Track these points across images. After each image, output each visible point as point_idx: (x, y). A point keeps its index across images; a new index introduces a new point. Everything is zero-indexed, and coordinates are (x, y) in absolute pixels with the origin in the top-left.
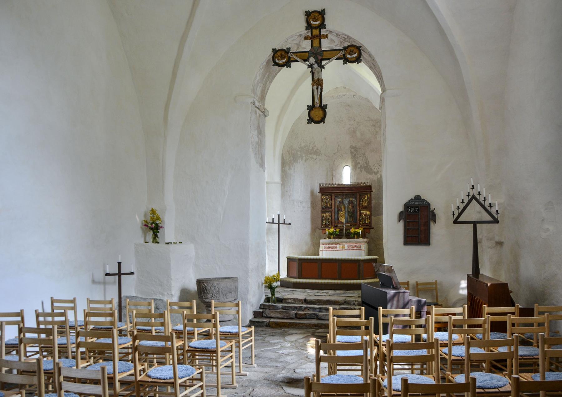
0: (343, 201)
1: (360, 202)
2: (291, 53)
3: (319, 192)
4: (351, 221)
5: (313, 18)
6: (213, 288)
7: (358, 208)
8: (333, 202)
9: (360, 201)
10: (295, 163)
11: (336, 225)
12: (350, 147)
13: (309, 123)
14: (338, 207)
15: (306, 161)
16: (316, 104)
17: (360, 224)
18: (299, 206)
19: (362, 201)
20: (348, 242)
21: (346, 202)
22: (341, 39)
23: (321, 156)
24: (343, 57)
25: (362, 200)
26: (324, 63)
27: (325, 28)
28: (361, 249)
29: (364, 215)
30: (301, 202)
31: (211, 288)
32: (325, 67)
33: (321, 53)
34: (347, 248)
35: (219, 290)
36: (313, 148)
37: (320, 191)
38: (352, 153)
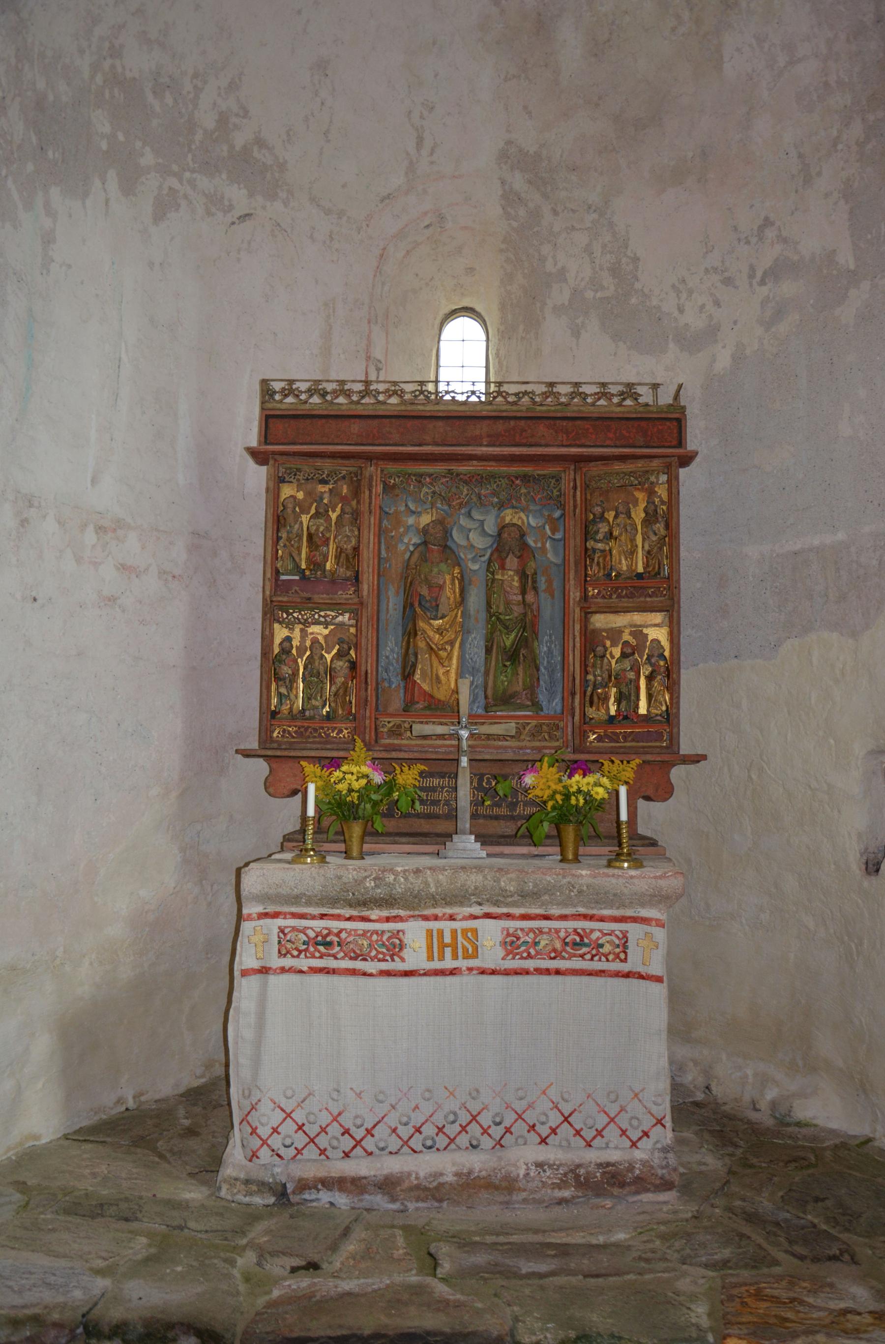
0: (447, 533)
1: (590, 544)
8: (369, 538)
9: (587, 535)
12: (503, 156)
15: (160, 212)
18: (79, 560)
19: (610, 536)
20: (503, 892)
23: (286, 204)
34: (501, 952)
36: (223, 120)
37: (266, 436)
38: (511, 198)
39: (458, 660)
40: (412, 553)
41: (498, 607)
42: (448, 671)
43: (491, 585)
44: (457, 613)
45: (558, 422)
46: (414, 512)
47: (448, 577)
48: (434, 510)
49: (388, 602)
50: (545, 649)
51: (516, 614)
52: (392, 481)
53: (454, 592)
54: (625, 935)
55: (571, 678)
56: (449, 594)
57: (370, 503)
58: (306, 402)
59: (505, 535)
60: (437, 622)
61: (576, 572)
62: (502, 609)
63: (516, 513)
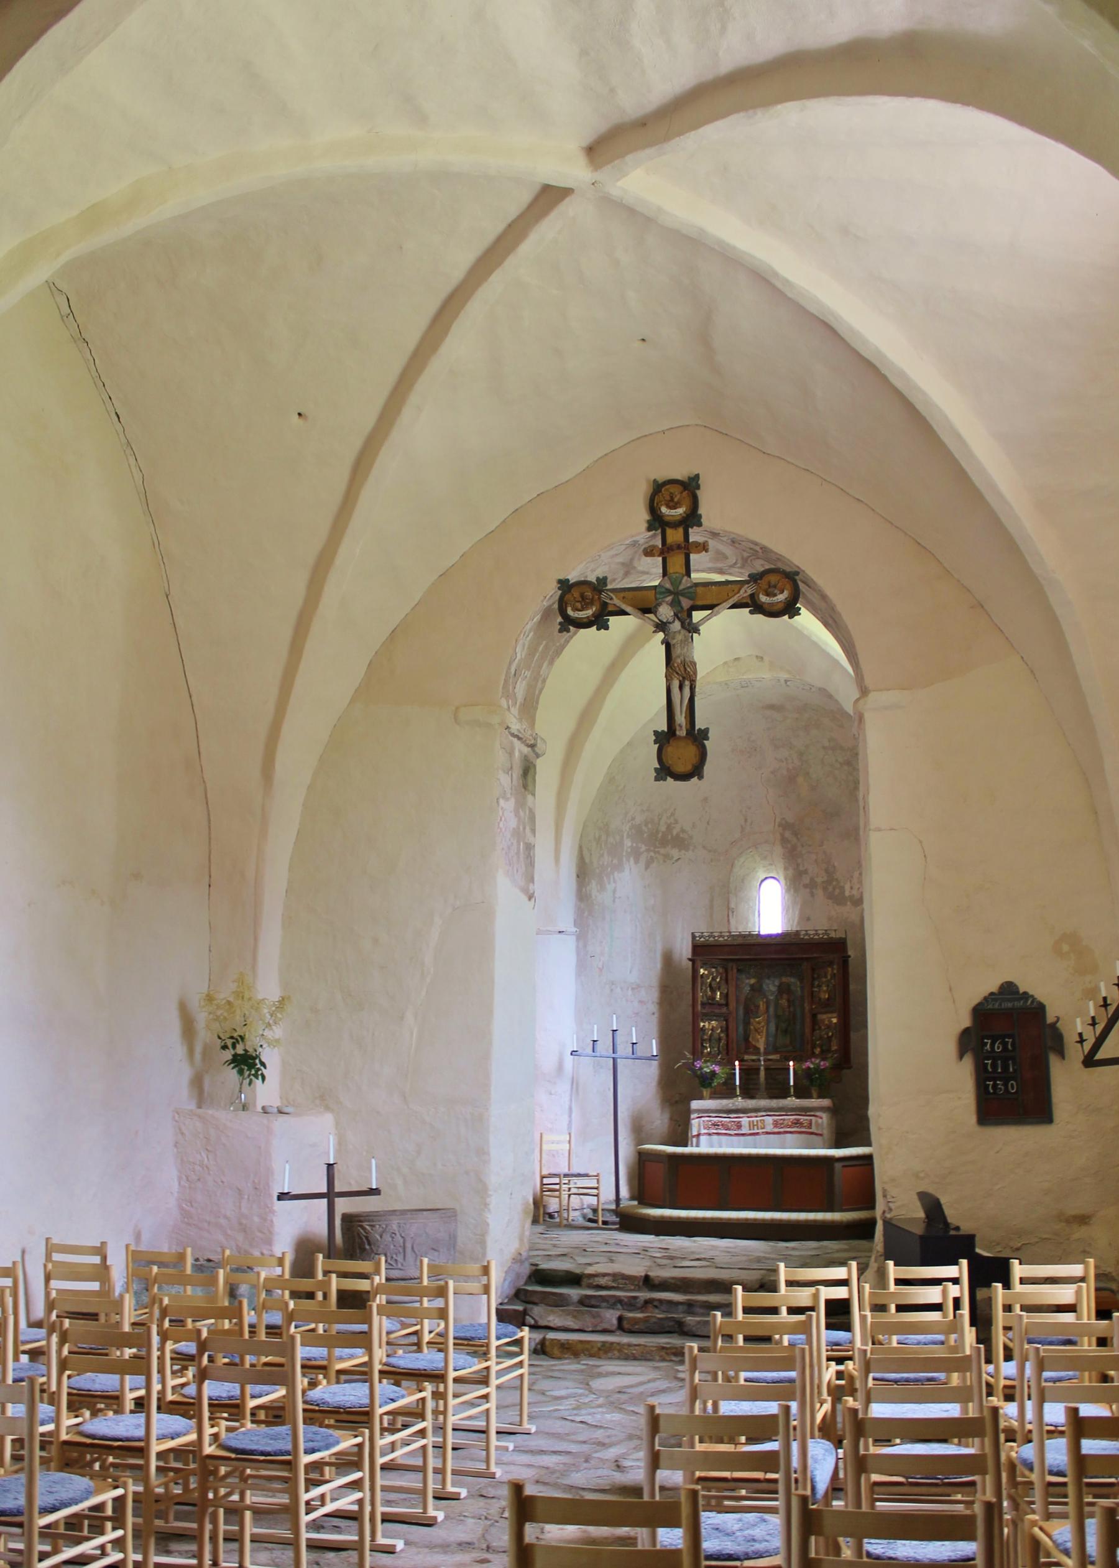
0: (761, 985)
2: (609, 593)
3: (690, 957)
5: (668, 498)
6: (387, 1237)
7: (807, 1006)
8: (732, 990)
10: (616, 874)
13: (659, 781)
16: (678, 728)
18: (627, 1001)
21: (771, 986)
22: (744, 551)
24: (750, 602)
26: (697, 616)
27: (700, 525)
28: (810, 1130)
29: (823, 1027)
30: (636, 988)
31: (381, 1237)
32: (701, 628)
33: (690, 590)
34: (772, 1126)
35: (404, 1243)
43: (777, 1005)
54: (811, 1120)
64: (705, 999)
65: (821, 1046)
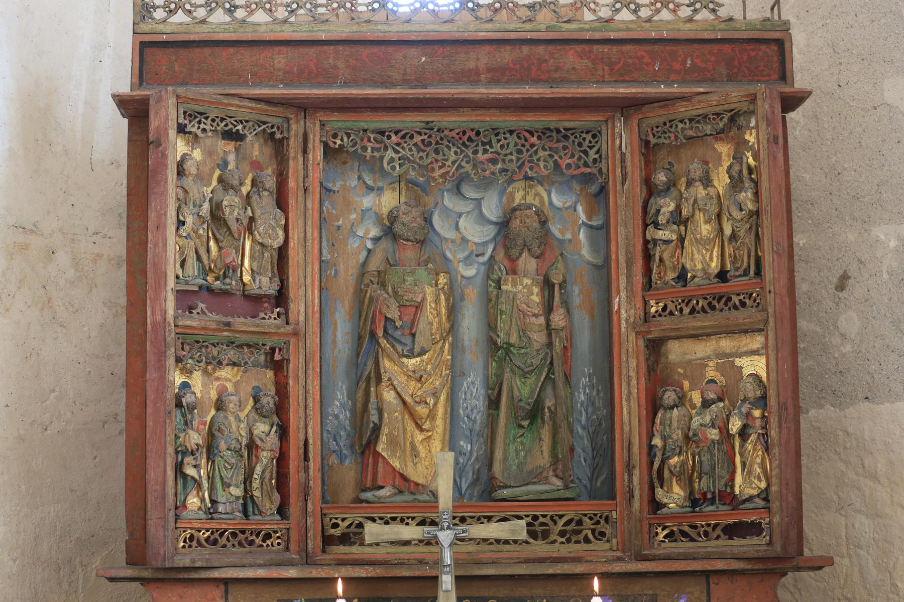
1: (651, 233)
4: (537, 476)
11: (345, 520)
14: (360, 292)
17: (656, 505)
25: (668, 206)
29: (696, 398)
39: (444, 419)
40: (369, 251)
41: (508, 334)
42: (429, 437)
44: (443, 346)
45: (595, 47)
46: (370, 189)
47: (429, 291)
48: (402, 184)
49: (335, 329)
50: (582, 397)
51: (536, 346)
52: (339, 142)
53: (439, 314)
55: (626, 444)
56: (431, 317)
57: (306, 176)
58: (203, 21)
59: (516, 224)
60: (413, 361)
61: (629, 277)
62: (514, 339)
63: (531, 187)
64: (192, 267)
65: (687, 478)
